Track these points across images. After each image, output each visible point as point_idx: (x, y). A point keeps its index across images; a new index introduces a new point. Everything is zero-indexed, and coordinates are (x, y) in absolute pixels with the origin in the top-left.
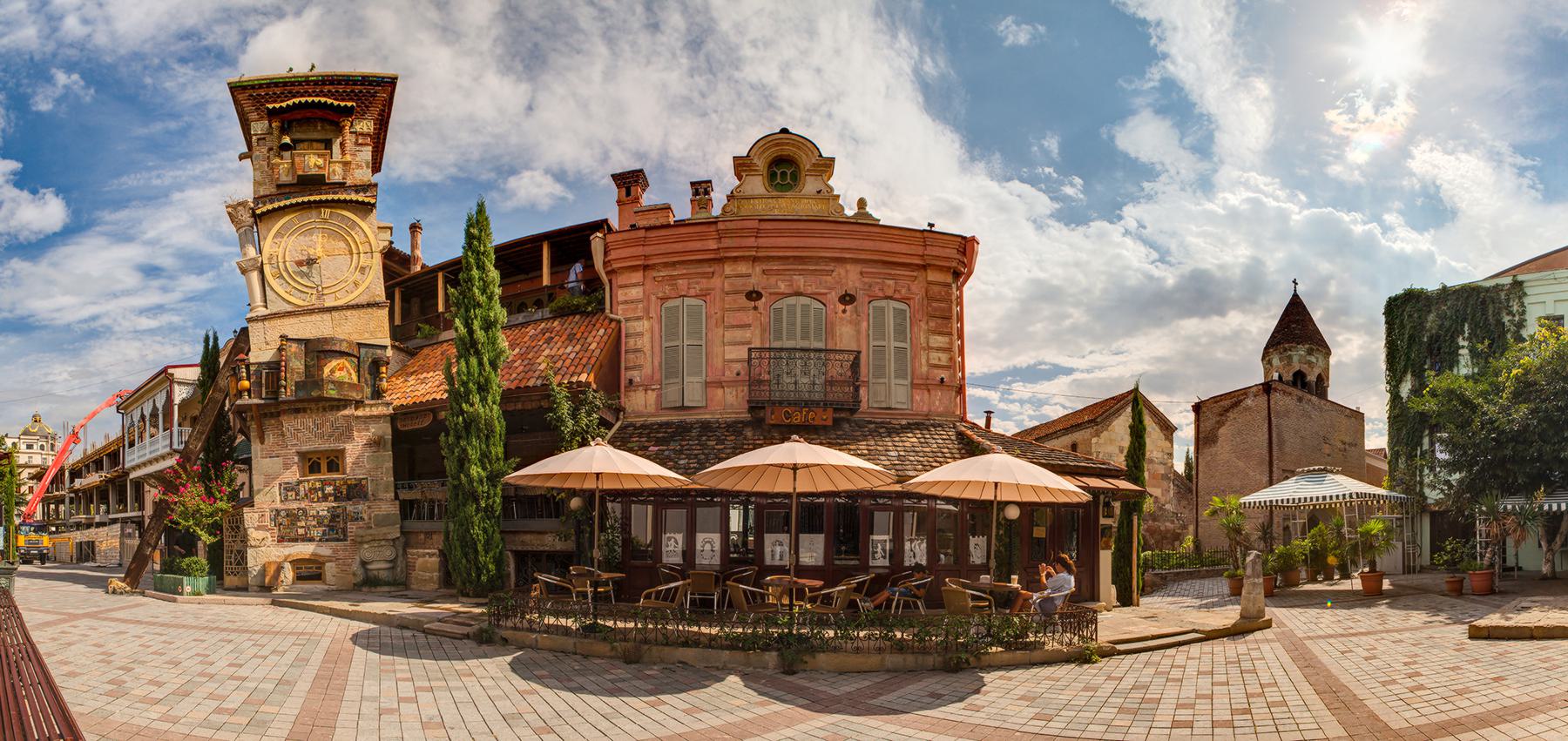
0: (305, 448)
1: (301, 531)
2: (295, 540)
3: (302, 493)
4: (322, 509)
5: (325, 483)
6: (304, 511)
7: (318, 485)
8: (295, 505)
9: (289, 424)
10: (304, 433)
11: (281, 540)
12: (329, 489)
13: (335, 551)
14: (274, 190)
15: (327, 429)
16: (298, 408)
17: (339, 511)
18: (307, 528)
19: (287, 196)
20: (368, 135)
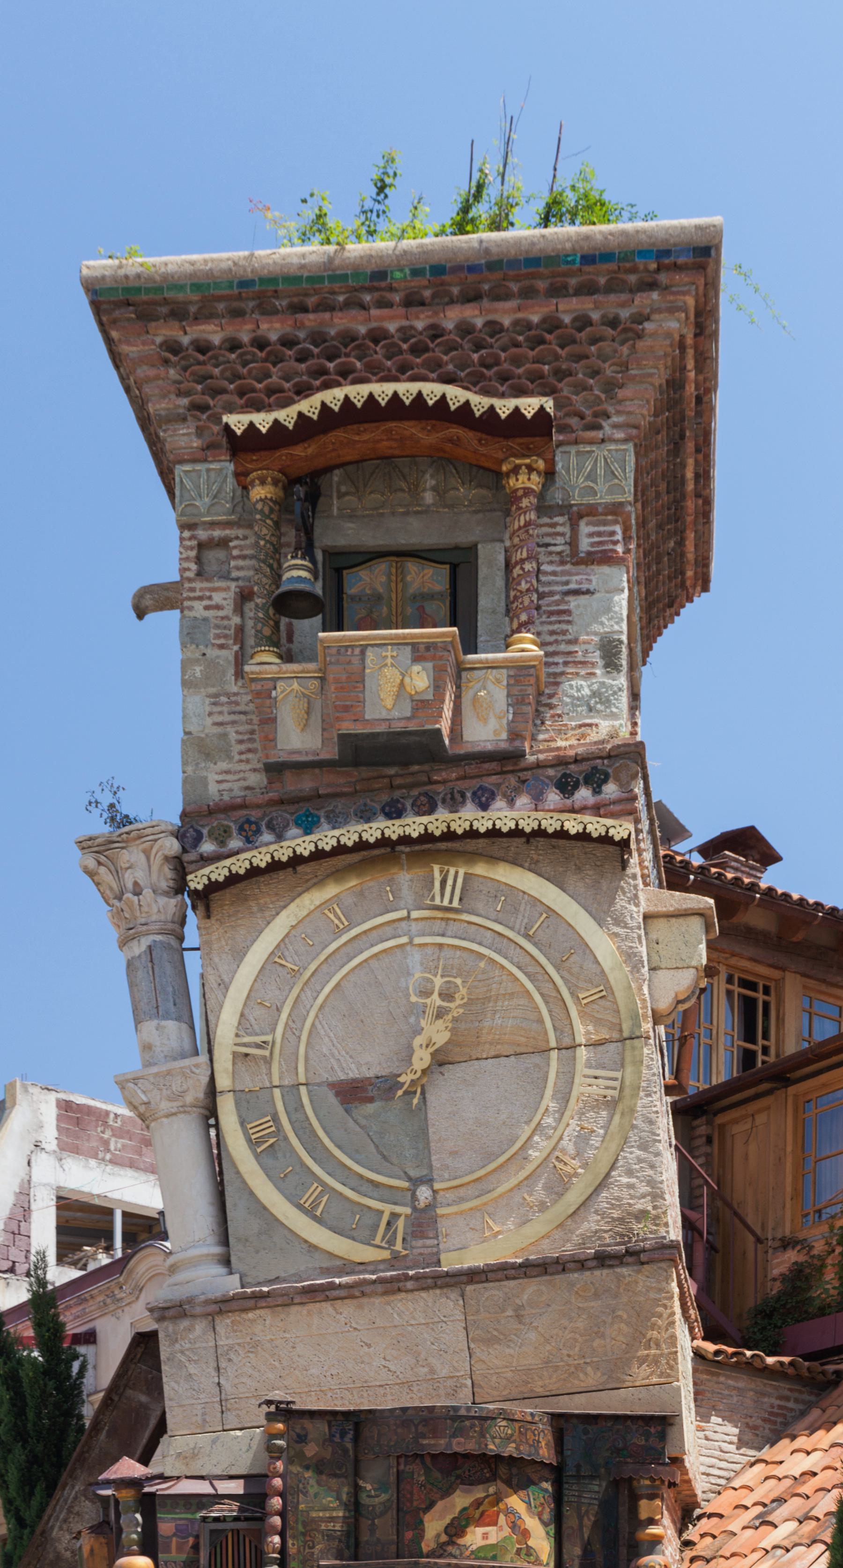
19: (307, 811)
20: (615, 509)
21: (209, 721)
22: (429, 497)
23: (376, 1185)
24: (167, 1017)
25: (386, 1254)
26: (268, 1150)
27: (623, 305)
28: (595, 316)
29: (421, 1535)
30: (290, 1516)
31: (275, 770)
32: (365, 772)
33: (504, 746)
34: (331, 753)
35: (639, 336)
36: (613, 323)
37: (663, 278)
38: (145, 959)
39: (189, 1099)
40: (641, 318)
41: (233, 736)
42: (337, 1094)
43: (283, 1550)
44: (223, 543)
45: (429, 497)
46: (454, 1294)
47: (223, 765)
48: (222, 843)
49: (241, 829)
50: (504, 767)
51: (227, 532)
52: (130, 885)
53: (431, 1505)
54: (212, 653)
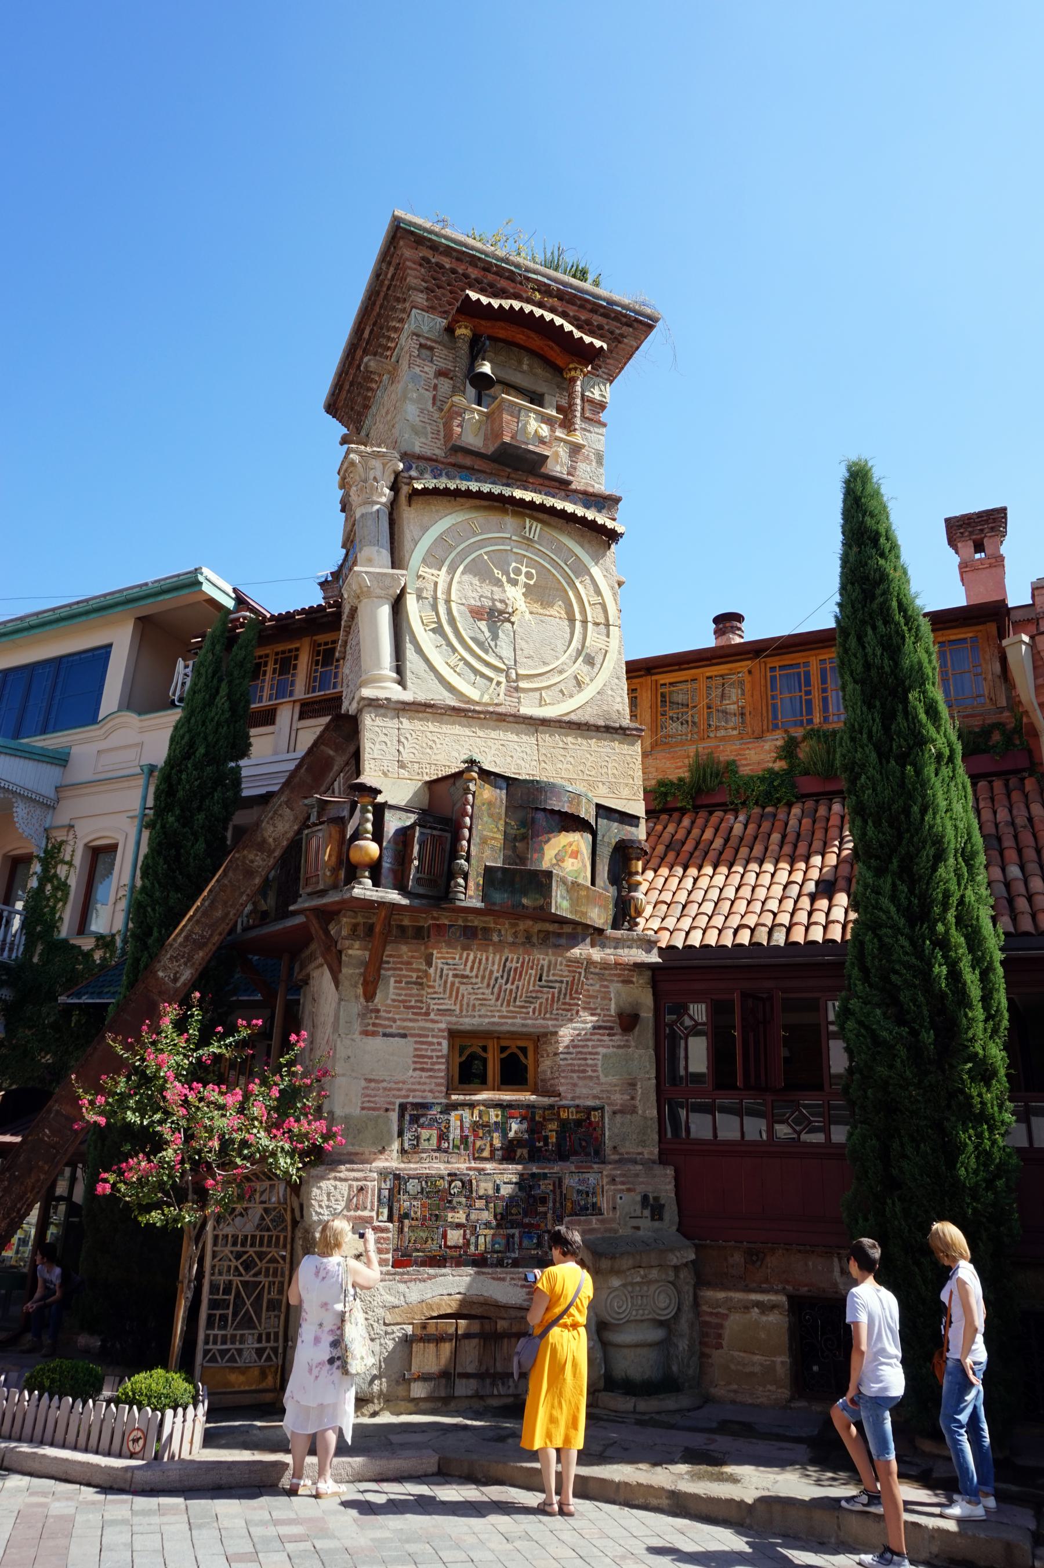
0: (468, 1022)
1: (455, 1237)
4: (503, 1178)
7: (494, 1116)
8: (438, 1167)
9: (447, 960)
10: (470, 986)
11: (402, 1260)
15: (527, 983)
16: (471, 933)
19: (470, 472)
21: (418, 419)
22: (525, 367)
24: (382, 547)
27: (617, 328)
28: (606, 327)
30: (474, 831)
31: (458, 449)
32: (496, 466)
34: (490, 450)
35: (620, 342)
36: (612, 333)
37: (635, 324)
39: (391, 592)
40: (622, 336)
41: (429, 429)
42: (470, 612)
44: (431, 349)
45: (525, 367)
47: (423, 440)
48: (421, 474)
49: (432, 471)
51: (433, 344)
52: (372, 477)
54: (422, 391)
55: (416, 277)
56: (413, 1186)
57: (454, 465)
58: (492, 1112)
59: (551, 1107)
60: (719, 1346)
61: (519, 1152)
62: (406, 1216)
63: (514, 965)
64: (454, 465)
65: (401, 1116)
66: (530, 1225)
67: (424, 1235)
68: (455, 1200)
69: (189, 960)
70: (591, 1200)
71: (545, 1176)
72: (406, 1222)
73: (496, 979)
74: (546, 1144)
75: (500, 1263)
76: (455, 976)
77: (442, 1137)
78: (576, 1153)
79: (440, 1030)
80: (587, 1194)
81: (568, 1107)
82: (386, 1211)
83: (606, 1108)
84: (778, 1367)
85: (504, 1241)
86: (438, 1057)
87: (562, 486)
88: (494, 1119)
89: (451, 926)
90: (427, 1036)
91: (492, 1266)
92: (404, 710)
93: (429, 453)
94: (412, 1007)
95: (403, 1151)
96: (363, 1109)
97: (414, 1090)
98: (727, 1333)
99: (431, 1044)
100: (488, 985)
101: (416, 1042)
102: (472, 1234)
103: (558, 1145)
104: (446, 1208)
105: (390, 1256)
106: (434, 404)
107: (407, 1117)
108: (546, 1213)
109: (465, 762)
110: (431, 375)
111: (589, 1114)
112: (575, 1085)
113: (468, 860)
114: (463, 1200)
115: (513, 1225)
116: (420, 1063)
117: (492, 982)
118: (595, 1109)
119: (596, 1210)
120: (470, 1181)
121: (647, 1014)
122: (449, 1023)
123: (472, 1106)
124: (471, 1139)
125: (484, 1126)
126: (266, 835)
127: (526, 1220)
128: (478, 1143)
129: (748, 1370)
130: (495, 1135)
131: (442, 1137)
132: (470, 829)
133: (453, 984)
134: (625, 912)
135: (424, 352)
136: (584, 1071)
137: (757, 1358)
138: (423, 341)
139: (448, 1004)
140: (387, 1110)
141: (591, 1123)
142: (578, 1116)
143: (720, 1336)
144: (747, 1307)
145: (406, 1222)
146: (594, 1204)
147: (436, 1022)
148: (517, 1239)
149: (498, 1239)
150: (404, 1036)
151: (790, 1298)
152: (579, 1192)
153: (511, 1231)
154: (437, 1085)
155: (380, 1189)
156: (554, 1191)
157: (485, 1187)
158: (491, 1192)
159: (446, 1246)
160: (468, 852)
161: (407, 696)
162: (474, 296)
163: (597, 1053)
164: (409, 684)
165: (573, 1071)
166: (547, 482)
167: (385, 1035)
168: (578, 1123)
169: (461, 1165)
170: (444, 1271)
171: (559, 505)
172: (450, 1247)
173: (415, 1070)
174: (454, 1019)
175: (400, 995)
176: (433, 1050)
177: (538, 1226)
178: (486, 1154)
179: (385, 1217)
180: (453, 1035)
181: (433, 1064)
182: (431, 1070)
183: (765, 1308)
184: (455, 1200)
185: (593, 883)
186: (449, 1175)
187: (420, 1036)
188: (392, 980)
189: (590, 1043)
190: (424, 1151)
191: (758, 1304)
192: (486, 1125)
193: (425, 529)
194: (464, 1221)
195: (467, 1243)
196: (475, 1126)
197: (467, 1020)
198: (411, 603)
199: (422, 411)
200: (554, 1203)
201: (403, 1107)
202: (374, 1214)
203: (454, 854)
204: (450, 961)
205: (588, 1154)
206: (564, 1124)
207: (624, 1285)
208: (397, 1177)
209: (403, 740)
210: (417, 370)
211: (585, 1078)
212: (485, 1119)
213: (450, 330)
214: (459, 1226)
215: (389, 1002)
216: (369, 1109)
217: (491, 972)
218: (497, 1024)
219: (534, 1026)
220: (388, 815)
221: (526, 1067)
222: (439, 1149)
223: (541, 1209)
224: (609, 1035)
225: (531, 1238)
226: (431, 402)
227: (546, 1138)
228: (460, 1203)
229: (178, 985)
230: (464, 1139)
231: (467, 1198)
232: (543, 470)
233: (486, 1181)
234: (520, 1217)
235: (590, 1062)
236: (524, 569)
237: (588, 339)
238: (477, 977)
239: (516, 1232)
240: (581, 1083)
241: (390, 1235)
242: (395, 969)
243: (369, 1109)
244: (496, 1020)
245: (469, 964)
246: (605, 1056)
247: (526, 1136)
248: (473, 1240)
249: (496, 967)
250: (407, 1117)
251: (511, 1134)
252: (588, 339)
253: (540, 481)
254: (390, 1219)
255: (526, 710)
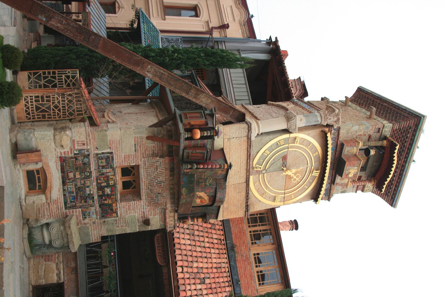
1: (71, 175)
2: (63, 171)
3: (104, 171)
5: (113, 187)
6: (89, 177)
7: (111, 182)
8: (93, 167)
11: (63, 160)
12: (108, 191)
13: (56, 202)
14: (341, 139)
15: (157, 189)
17: (90, 202)
18: (75, 179)
23: (267, 163)
25: (254, 166)
26: (277, 145)
29: (199, 192)
31: (342, 145)
33: (336, 182)
34: (343, 157)
38: (317, 120)
43: (199, 168)
44: (379, 132)
46: (245, 181)
50: (332, 182)
51: (380, 132)
53: (206, 193)
54: (363, 131)
55: (404, 125)
56: (86, 160)
57: (337, 145)
58: (113, 182)
59: (116, 200)
60: (45, 261)
61: (101, 192)
62: (76, 159)
63: (162, 185)
64: (337, 145)
65: (109, 153)
66: (77, 199)
67: (71, 165)
68: (83, 174)
69: (155, 75)
70: (87, 216)
71: (93, 201)
72: (74, 159)
73: (157, 179)
74: (104, 200)
75: (64, 190)
76: (157, 166)
77: (103, 167)
78: (102, 210)
79: (138, 163)
80: (89, 215)
81: (117, 206)
82: (77, 152)
83: (117, 218)
84: (41, 281)
85: (71, 191)
86: (129, 163)
87: (332, 182)
88: (110, 182)
89: (174, 163)
90: (136, 158)
91: (63, 188)
92: (248, 138)
93: (340, 136)
94: (145, 152)
95: (97, 154)
96: (110, 140)
97: (117, 156)
98: (50, 263)
99: (133, 160)
100: (155, 177)
101: (133, 155)
102: (73, 181)
103: (104, 204)
104: (80, 171)
105: (63, 155)
106: (359, 135)
107: (108, 155)
108: (81, 203)
109: (230, 164)
110: (369, 133)
111: (115, 213)
112: (124, 207)
113: (197, 168)
114: (83, 177)
115: (77, 193)
116: (128, 157)
117: (156, 178)
118: (117, 214)
119: (84, 218)
120: (89, 178)
121: (149, 228)
122: (141, 165)
123: (114, 175)
124: (103, 176)
125: (108, 179)
126: (201, 95)
127: (79, 197)
128: (102, 179)
129: (40, 271)
130: (106, 184)
131: (103, 167)
132: (207, 168)
133: (154, 165)
134: (183, 218)
135: (378, 130)
136: (129, 210)
137: (43, 273)
138: (381, 129)
139: (147, 164)
140: (110, 148)
141: (112, 213)
142: (114, 209)
143: (49, 260)
144: (58, 269)
145: (74, 159)
146: (86, 218)
147: (141, 160)
148: (72, 195)
149: (72, 189)
150: (135, 151)
151: (63, 283)
152: (89, 213)
153: (75, 193)
154: (120, 163)
155: (84, 150)
156: (89, 205)
157: (88, 183)
158: (87, 185)
159: (68, 173)
160: (199, 168)
161: (253, 138)
162: (397, 147)
163: (135, 213)
164: (257, 138)
165: (129, 206)
166: (333, 176)
167: (135, 145)
168: (112, 210)
169: (94, 175)
170: (60, 172)
171: (325, 182)
172: (68, 174)
173: (125, 156)
174: (142, 166)
175: (149, 148)
176: (131, 161)
177: (77, 201)
178: (99, 181)
179: (75, 152)
180: (138, 167)
181: (127, 161)
182: (125, 161)
183: (58, 275)
184: (83, 174)
185: (193, 207)
186: (91, 171)
187: (136, 156)
188: (154, 145)
189: (138, 211)
190: (98, 162)
191: (60, 273)
192: (108, 181)
193: (314, 137)
194: (77, 177)
195: (69, 179)
196: (108, 177)
197: (142, 170)
198: (286, 136)
199: (356, 132)
200: (85, 205)
201: (112, 153)
202: (76, 149)
203: (198, 163)
204: (162, 164)
205: (102, 213)
206: (111, 205)
207: (61, 231)
208: (89, 155)
209: (238, 139)
210: (371, 128)
211: (127, 210)
212: (110, 180)
213: (385, 138)
214: (75, 176)
215: (146, 145)
216: (110, 142)
217: (159, 178)
218: (142, 181)
219: (143, 192)
220: (209, 140)
221: (129, 189)
222: (99, 166)
223: (83, 201)
224: (142, 217)
225: (73, 199)
226: (359, 134)
227: (106, 200)
228: (82, 175)
229: (146, 73)
230: (103, 174)
231: (84, 178)
232: (337, 175)
233: (90, 183)
234: (79, 195)
235: (132, 211)
236: (297, 179)
237: (385, 186)
238: (157, 173)
239: (75, 194)
240: (125, 209)
241: (70, 155)
242: (158, 145)
243: (110, 142)
244: (143, 180)
245: (162, 170)
246: (135, 216)
247: (106, 193)
248: (71, 181)
249: (161, 179)
250: (108, 155)
251: (106, 189)
252: (385, 186)
253: (334, 174)
254: (75, 154)
255: (251, 177)
